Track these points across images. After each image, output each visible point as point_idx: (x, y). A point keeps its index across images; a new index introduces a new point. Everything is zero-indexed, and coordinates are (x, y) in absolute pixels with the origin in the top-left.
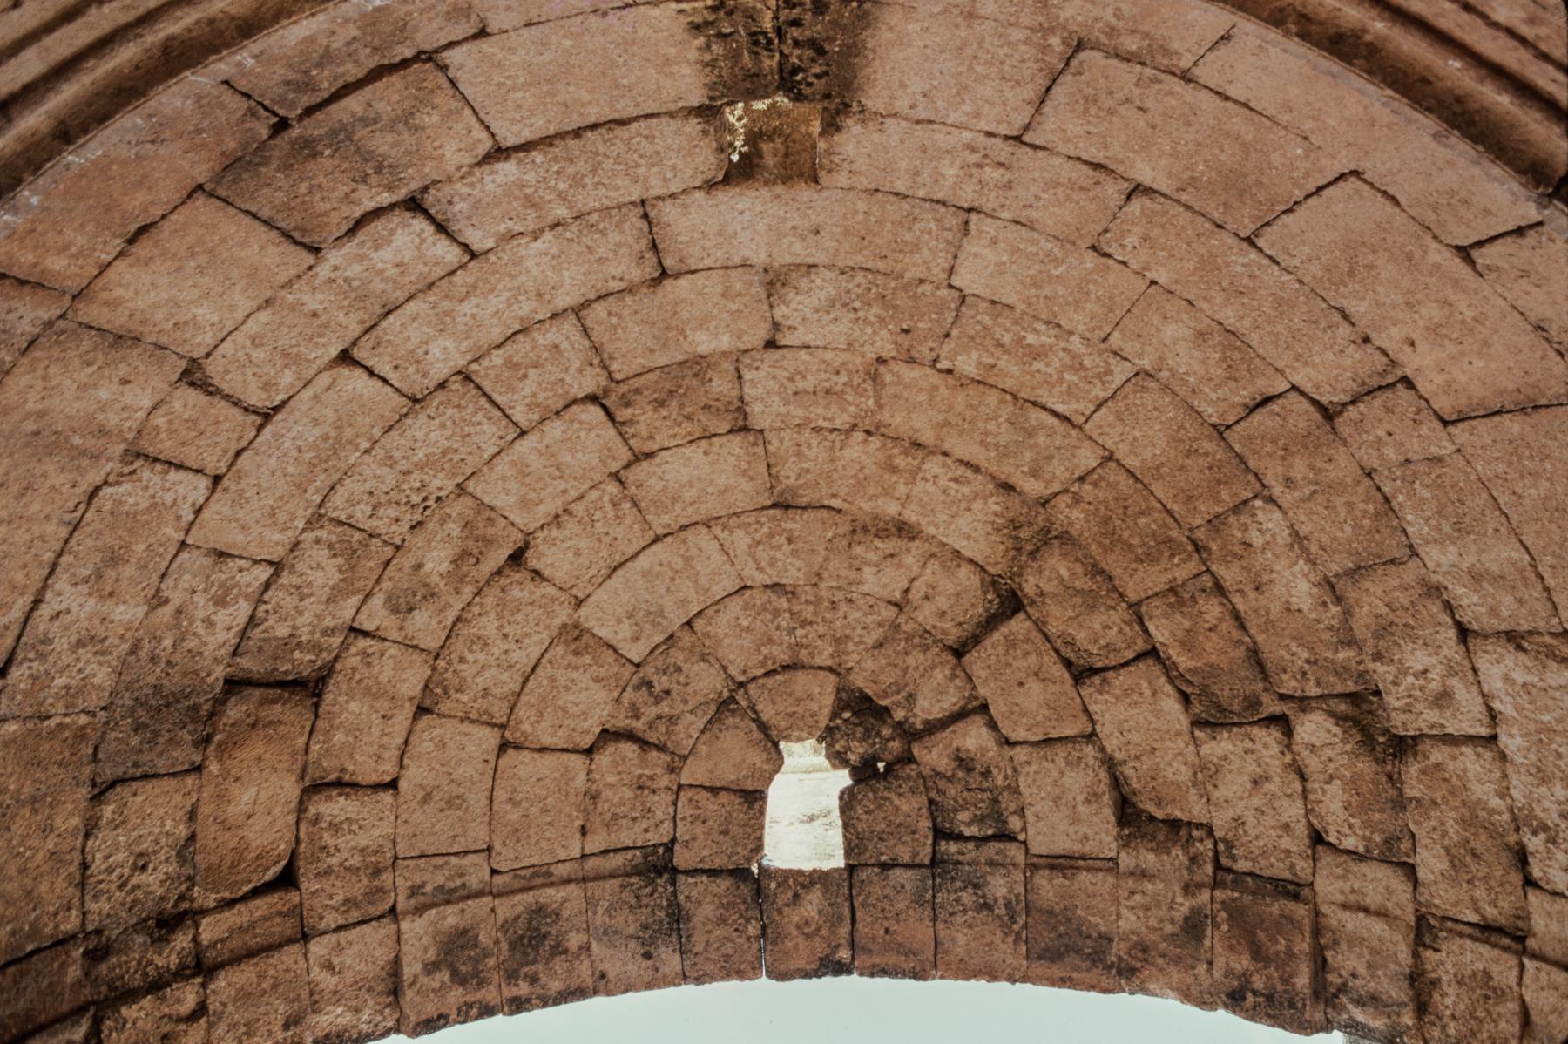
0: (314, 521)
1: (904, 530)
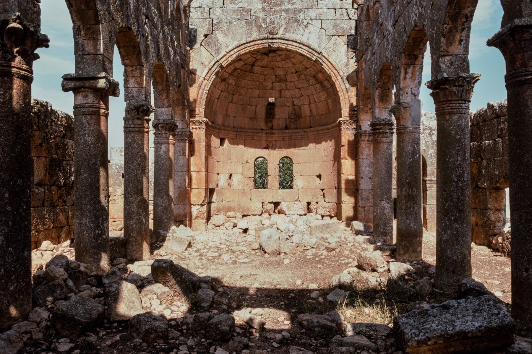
1: (262, 67)
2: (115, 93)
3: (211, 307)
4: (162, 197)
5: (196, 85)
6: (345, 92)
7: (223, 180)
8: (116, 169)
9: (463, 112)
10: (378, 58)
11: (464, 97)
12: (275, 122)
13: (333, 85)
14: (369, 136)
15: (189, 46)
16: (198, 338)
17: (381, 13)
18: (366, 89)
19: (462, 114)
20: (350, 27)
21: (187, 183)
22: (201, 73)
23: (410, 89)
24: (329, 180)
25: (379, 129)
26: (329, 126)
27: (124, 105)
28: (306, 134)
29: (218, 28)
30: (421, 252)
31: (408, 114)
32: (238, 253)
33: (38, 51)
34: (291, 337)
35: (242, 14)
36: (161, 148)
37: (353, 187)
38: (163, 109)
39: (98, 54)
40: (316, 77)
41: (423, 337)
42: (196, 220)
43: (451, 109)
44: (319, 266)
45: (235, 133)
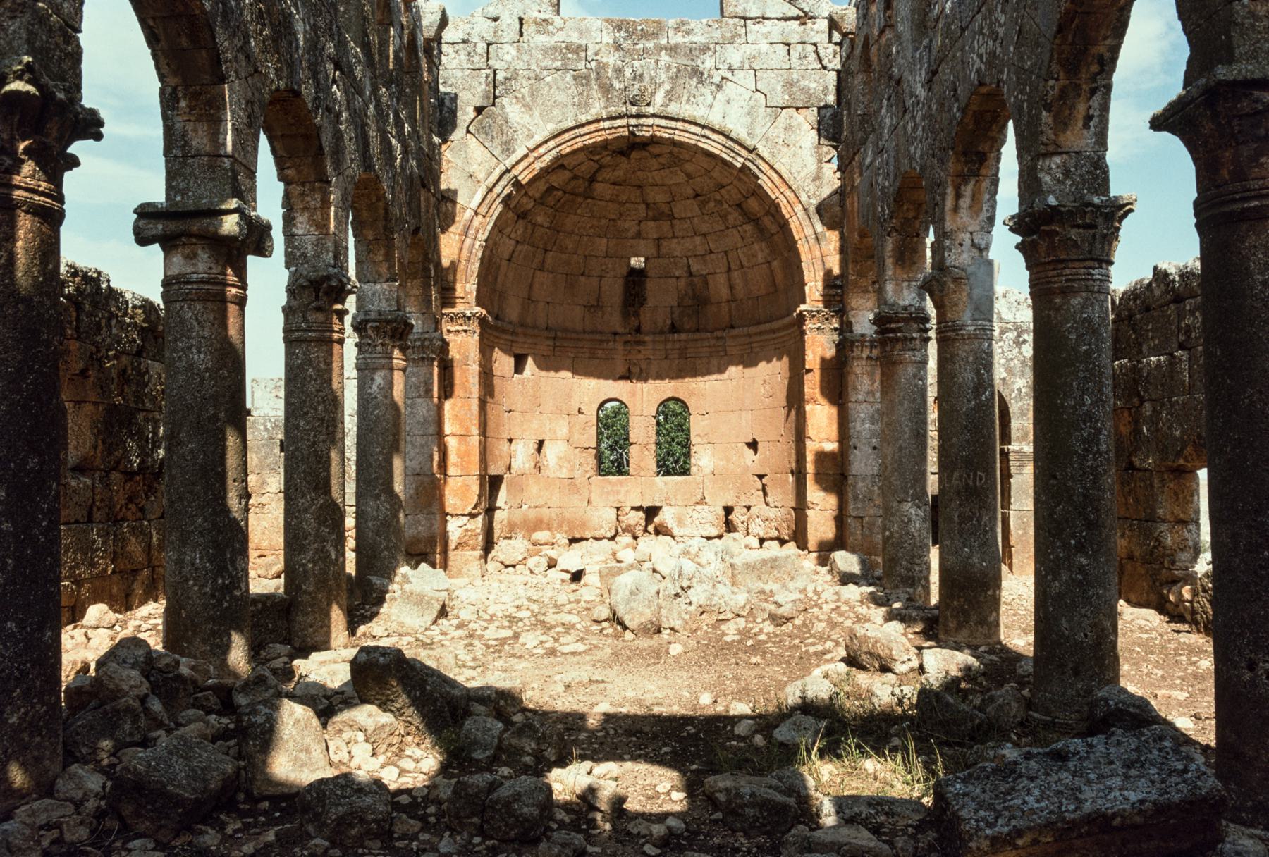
1: (614, 184)
2: (262, 249)
3: (495, 760)
4: (377, 497)
5: (456, 229)
6: (812, 241)
7: (521, 456)
8: (266, 429)
9: (1096, 289)
10: (892, 160)
11: (1097, 252)
12: (646, 316)
13: (784, 226)
14: (872, 347)
15: (439, 135)
16: (465, 835)
17: (898, 52)
18: (863, 235)
19: (1092, 292)
20: (824, 86)
21: (435, 464)
22: (469, 199)
23: (968, 235)
24: (777, 453)
25: (896, 330)
26: (775, 325)
27: (283, 276)
28: (720, 343)
29: (507, 92)
30: (998, 625)
31: (965, 294)
32: (560, 629)
33: (76, 148)
34: (687, 830)
35: (564, 59)
36: (373, 379)
37: (835, 472)
38: (378, 286)
39: (220, 156)
40: (744, 206)
41: (1006, 829)
42: (459, 552)
43: (1067, 280)
44: (754, 660)
45: (551, 343)
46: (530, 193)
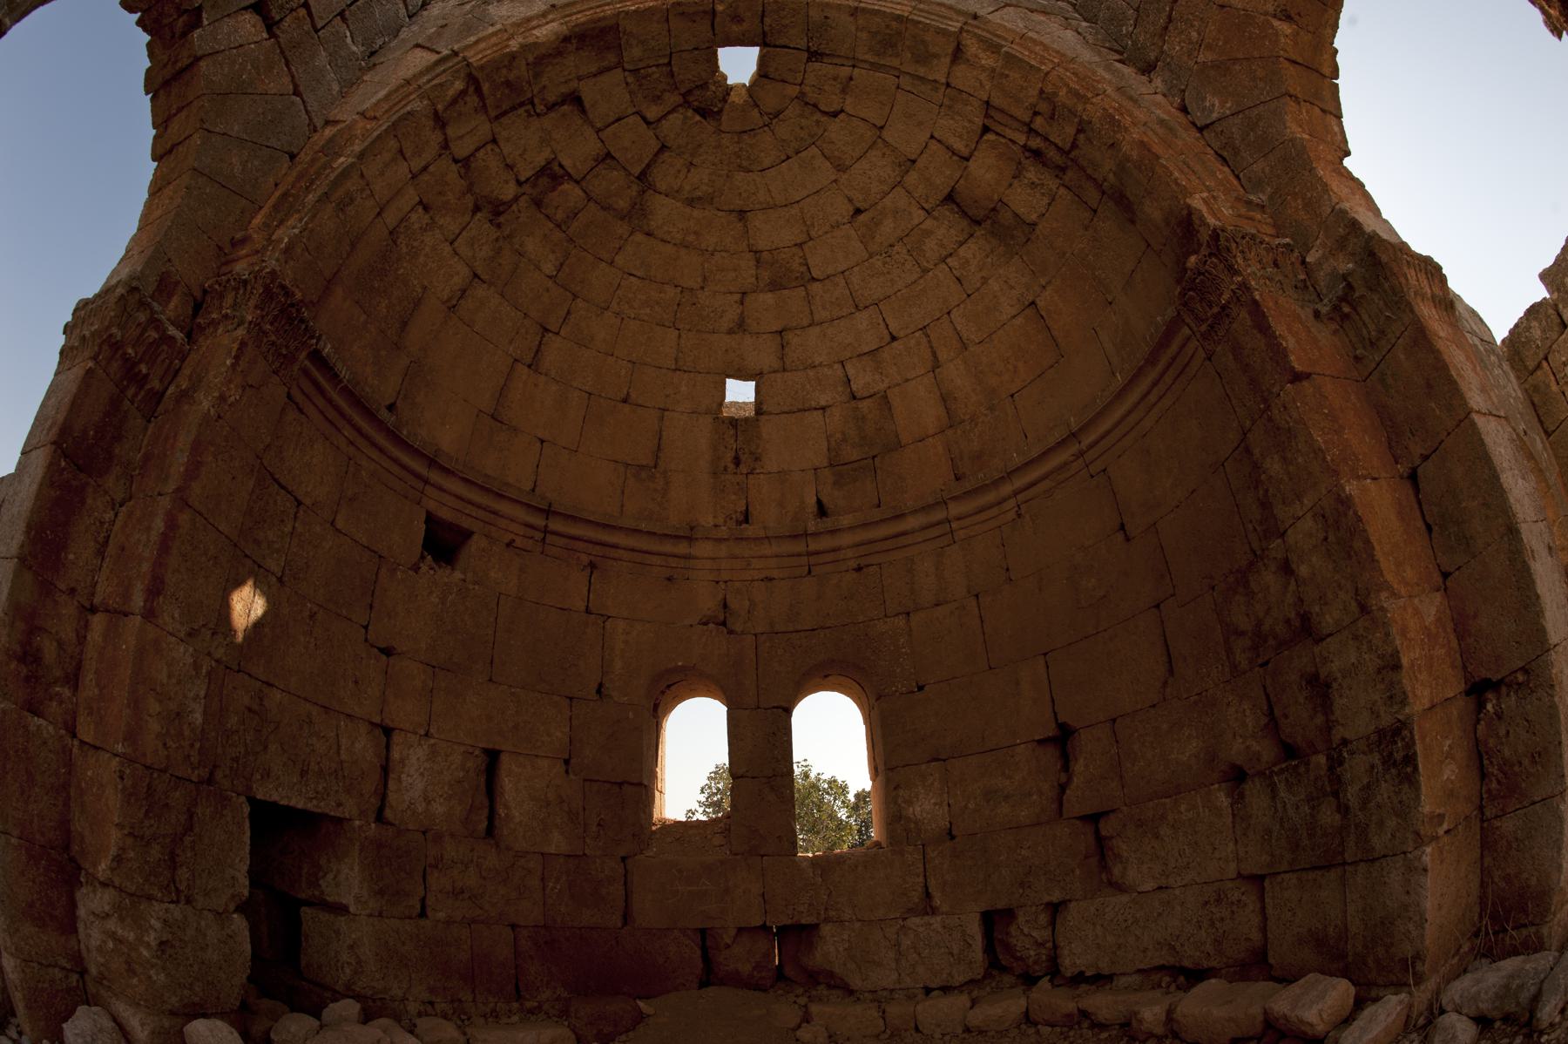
0: (925, 271)
1: (690, 202)
45: (539, 521)
46: (507, 149)
